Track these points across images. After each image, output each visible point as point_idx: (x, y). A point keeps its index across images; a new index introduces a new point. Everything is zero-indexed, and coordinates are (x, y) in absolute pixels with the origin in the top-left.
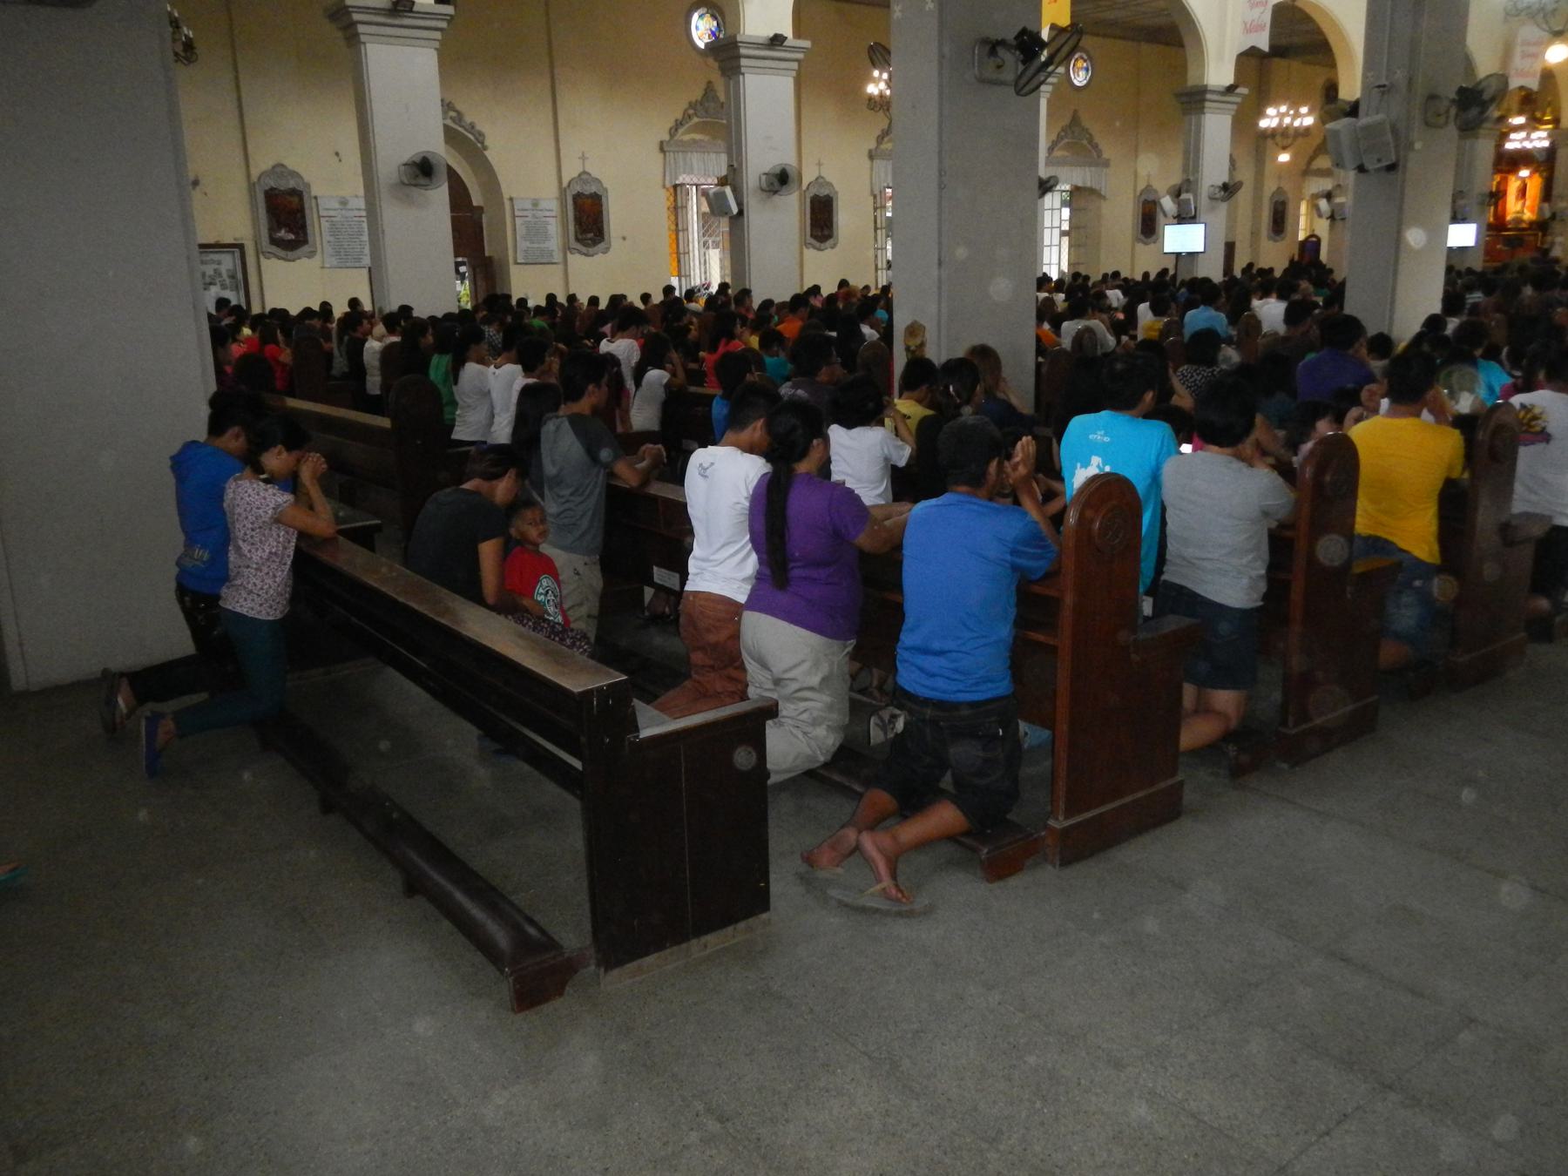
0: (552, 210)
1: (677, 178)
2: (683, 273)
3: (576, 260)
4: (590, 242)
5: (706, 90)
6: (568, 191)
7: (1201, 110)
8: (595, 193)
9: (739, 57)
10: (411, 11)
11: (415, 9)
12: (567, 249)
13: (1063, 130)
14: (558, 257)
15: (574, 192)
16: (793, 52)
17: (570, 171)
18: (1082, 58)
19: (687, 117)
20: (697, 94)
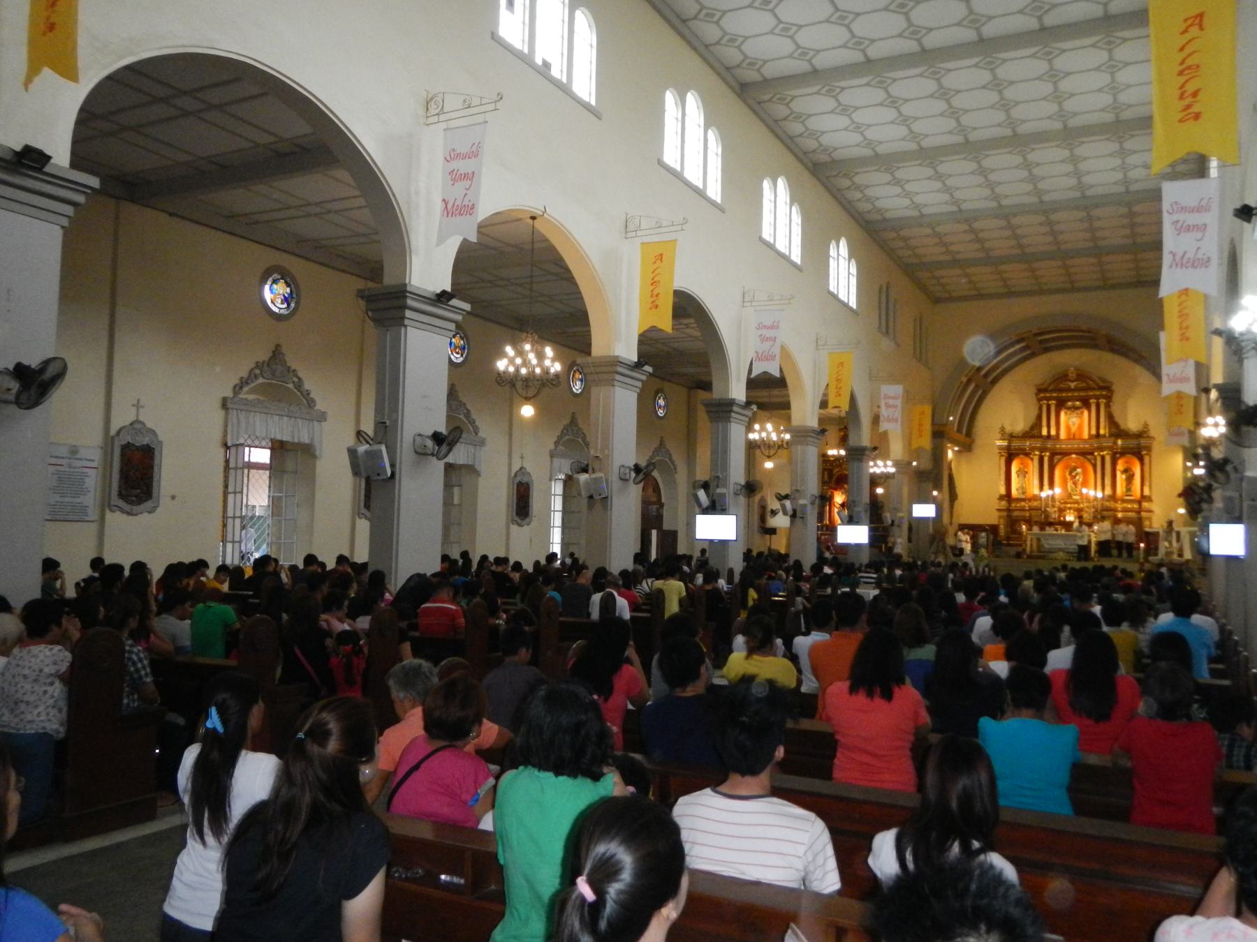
0: (93, 461)
1: (238, 440)
2: (229, 538)
3: (116, 520)
4: (134, 499)
5: (274, 352)
6: (116, 439)
7: (728, 420)
8: (148, 445)
9: (405, 307)
10: (40, 170)
11: (47, 169)
12: (106, 505)
13: (564, 428)
14: (93, 514)
15: (124, 443)
16: (454, 312)
17: (122, 418)
18: (578, 371)
19: (252, 376)
20: (263, 355)
